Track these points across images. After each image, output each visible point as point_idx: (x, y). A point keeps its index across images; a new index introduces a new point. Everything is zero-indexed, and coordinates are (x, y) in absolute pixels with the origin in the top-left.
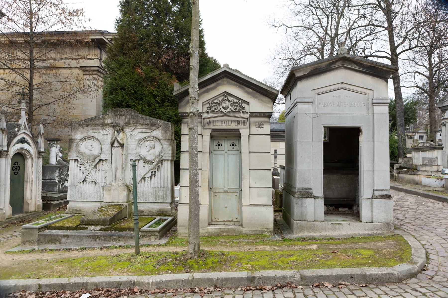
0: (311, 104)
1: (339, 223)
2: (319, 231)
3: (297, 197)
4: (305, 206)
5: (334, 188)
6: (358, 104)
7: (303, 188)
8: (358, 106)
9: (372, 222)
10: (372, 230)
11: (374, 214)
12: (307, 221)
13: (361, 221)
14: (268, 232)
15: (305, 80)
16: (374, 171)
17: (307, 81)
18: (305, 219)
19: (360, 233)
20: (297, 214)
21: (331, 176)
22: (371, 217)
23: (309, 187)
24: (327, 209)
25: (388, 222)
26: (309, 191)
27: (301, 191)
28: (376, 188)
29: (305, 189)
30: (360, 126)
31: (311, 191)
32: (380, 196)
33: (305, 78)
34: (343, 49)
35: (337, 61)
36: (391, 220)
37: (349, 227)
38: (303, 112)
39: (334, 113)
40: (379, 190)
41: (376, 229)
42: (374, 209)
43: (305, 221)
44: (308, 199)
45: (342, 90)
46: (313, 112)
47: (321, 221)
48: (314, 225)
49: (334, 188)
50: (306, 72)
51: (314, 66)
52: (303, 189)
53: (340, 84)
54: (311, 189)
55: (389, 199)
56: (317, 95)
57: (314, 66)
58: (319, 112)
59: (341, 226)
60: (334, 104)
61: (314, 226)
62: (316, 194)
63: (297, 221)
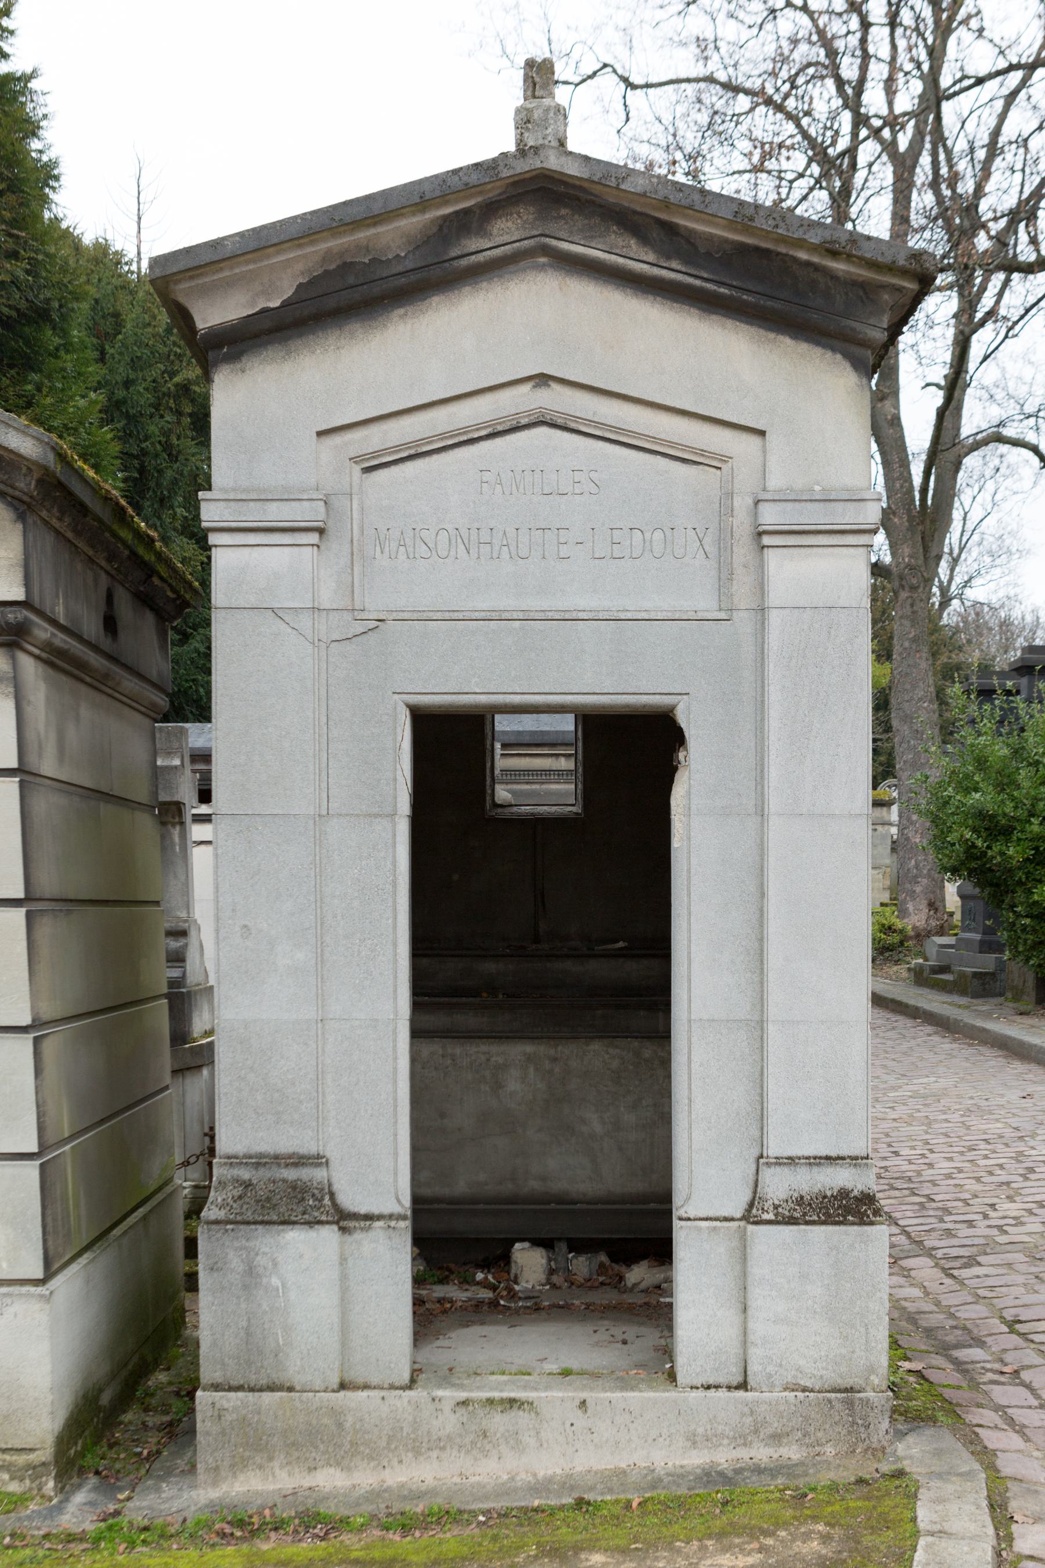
0: (313, 538)
1: (512, 1401)
2: (375, 1457)
3: (217, 1222)
4: (275, 1281)
5: (598, 1128)
6: (658, 535)
7: (261, 1155)
8: (658, 549)
9: (743, 1386)
10: (742, 1440)
11: (758, 1328)
12: (291, 1389)
13: (672, 1377)
14: (17, 1474)
15: (270, 352)
16: (761, 1024)
17: (287, 367)
18: (277, 1377)
19: (659, 1464)
20: (214, 1344)
21: (568, 1050)
22: (734, 1349)
23: (303, 1151)
24: (551, 1272)
25: (849, 1382)
26: (305, 1174)
27: (245, 1174)
28: (774, 1149)
29: (278, 1159)
30: (667, 700)
31: (319, 1174)
32: (800, 1201)
33: (264, 345)
34: (537, 115)
35: (491, 210)
36: (871, 1370)
37: (581, 1421)
38: (252, 600)
39: (484, 603)
40: (792, 1161)
41: (770, 1430)
42: (757, 1297)
43: (272, 1388)
44: (295, 1237)
45: (542, 432)
46: (327, 597)
47: (392, 1387)
48: (336, 1414)
49: (598, 1128)
50: (266, 293)
51: (323, 246)
52: (259, 1161)
53: (525, 388)
54: (318, 1160)
55: (862, 1223)
56: (357, 469)
57: (323, 246)
58: (375, 603)
59: (522, 1418)
60: (485, 536)
61: (340, 1425)
62: (351, 1199)
63: (216, 1387)
